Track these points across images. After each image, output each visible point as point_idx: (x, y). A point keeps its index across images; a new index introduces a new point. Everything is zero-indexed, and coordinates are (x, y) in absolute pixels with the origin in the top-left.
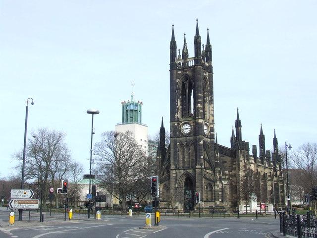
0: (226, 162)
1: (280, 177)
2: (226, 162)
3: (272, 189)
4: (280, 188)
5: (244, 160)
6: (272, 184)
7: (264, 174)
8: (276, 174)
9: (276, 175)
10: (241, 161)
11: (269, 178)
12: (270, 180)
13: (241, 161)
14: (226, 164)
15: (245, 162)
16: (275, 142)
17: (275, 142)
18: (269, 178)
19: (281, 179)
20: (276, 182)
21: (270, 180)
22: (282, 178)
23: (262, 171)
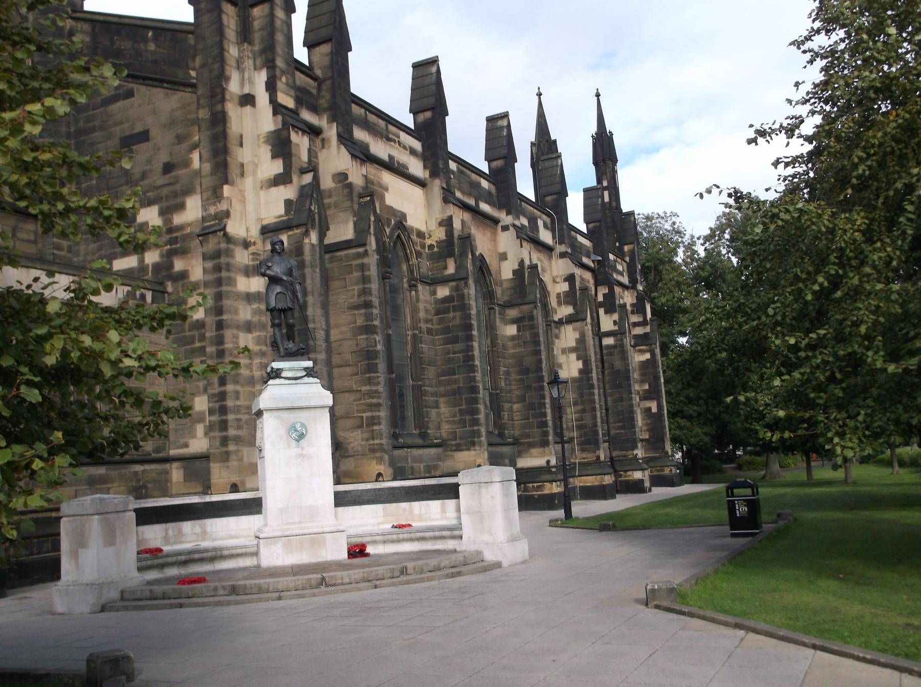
0: (144, 136)
1: (635, 318)
2: (144, 136)
3: (585, 371)
4: (636, 375)
5: (271, 87)
6: (581, 341)
7: (519, 273)
8: (610, 297)
9: (610, 305)
10: (248, 100)
11: (566, 311)
12: (570, 320)
13: (248, 100)
14: (143, 150)
15: (277, 108)
16: (604, 151)
17: (604, 151)
18: (566, 311)
19: (639, 331)
20: (608, 341)
21: (570, 320)
22: (644, 323)
23: (503, 257)
